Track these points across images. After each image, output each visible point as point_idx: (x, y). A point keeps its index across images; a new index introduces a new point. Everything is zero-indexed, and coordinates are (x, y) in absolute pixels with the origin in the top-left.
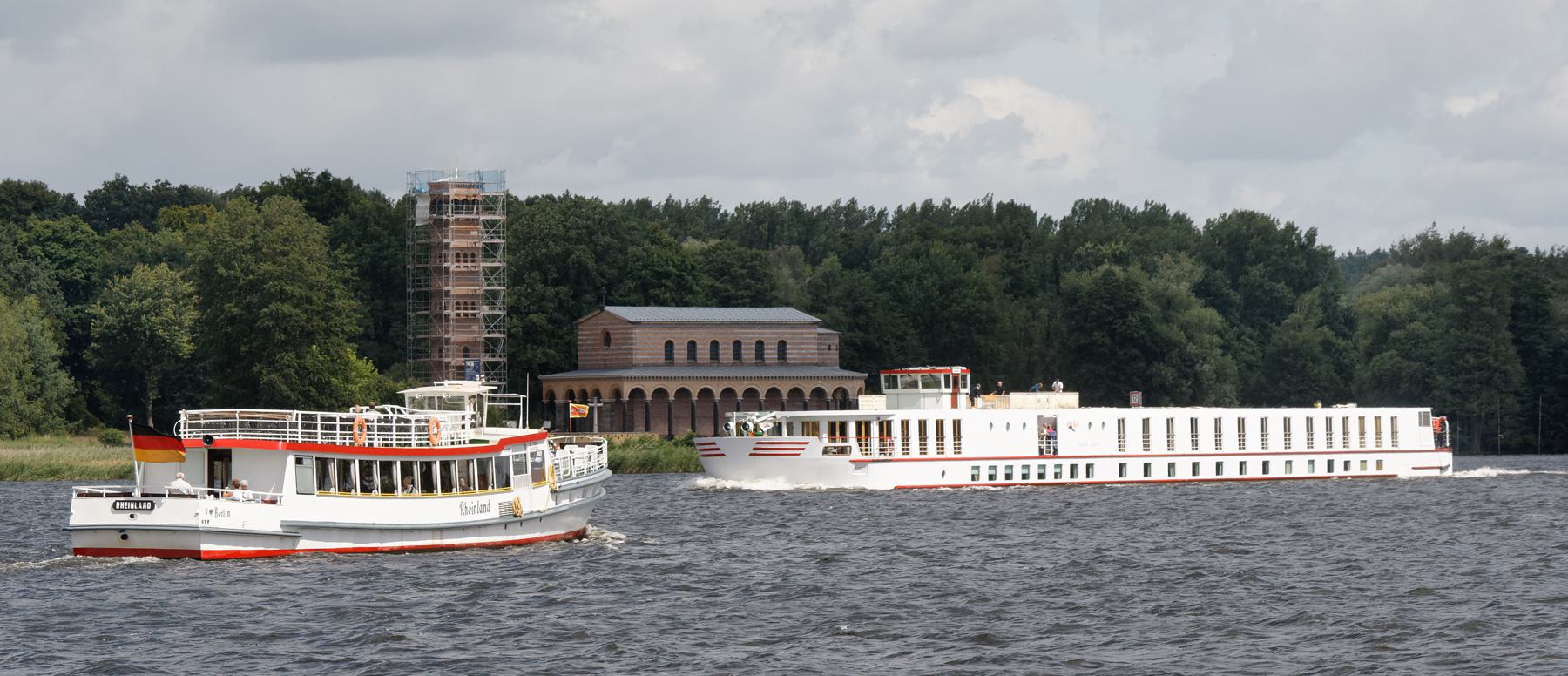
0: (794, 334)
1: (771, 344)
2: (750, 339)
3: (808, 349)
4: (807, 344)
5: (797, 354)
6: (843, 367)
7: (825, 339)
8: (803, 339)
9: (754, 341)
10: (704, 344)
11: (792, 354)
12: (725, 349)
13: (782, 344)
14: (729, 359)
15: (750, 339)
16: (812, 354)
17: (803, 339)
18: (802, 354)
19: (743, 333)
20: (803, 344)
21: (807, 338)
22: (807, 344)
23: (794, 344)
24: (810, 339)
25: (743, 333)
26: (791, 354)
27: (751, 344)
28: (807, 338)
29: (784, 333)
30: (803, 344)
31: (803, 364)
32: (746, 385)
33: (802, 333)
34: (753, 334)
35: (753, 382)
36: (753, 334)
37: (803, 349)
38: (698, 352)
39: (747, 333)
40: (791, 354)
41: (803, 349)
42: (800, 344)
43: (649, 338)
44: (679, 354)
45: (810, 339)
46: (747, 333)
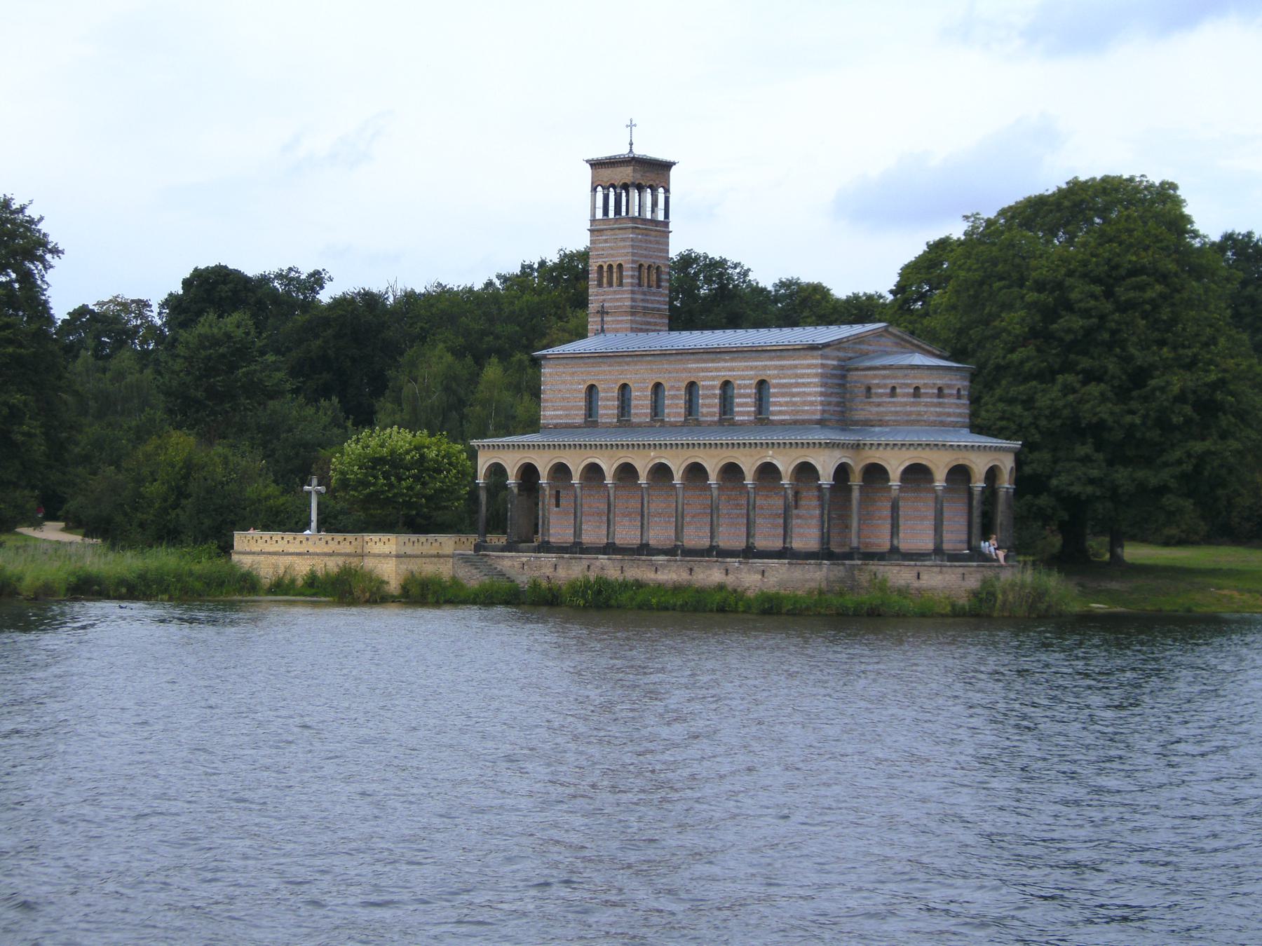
0: (782, 368)
1: (746, 387)
2: (713, 378)
3: (805, 394)
4: (804, 385)
5: (787, 404)
6: (976, 429)
7: (885, 377)
8: (797, 376)
9: (718, 383)
10: (642, 390)
11: (779, 407)
12: (674, 397)
13: (762, 385)
14: (679, 414)
15: (713, 378)
16: (812, 403)
17: (797, 376)
18: (794, 404)
19: (703, 370)
20: (797, 385)
21: (802, 376)
22: (804, 385)
23: (783, 386)
24: (808, 376)
25: (703, 370)
26: (775, 404)
27: (713, 387)
28: (802, 376)
29: (765, 368)
30: (797, 385)
31: (795, 422)
32: (655, 457)
33: (796, 367)
34: (717, 369)
35: (663, 452)
36: (717, 369)
37: (793, 395)
38: (634, 403)
39: (707, 370)
40: (775, 404)
41: (793, 395)
42: (791, 385)
43: (564, 382)
44: (606, 407)
45: (808, 376)
46: (707, 370)
